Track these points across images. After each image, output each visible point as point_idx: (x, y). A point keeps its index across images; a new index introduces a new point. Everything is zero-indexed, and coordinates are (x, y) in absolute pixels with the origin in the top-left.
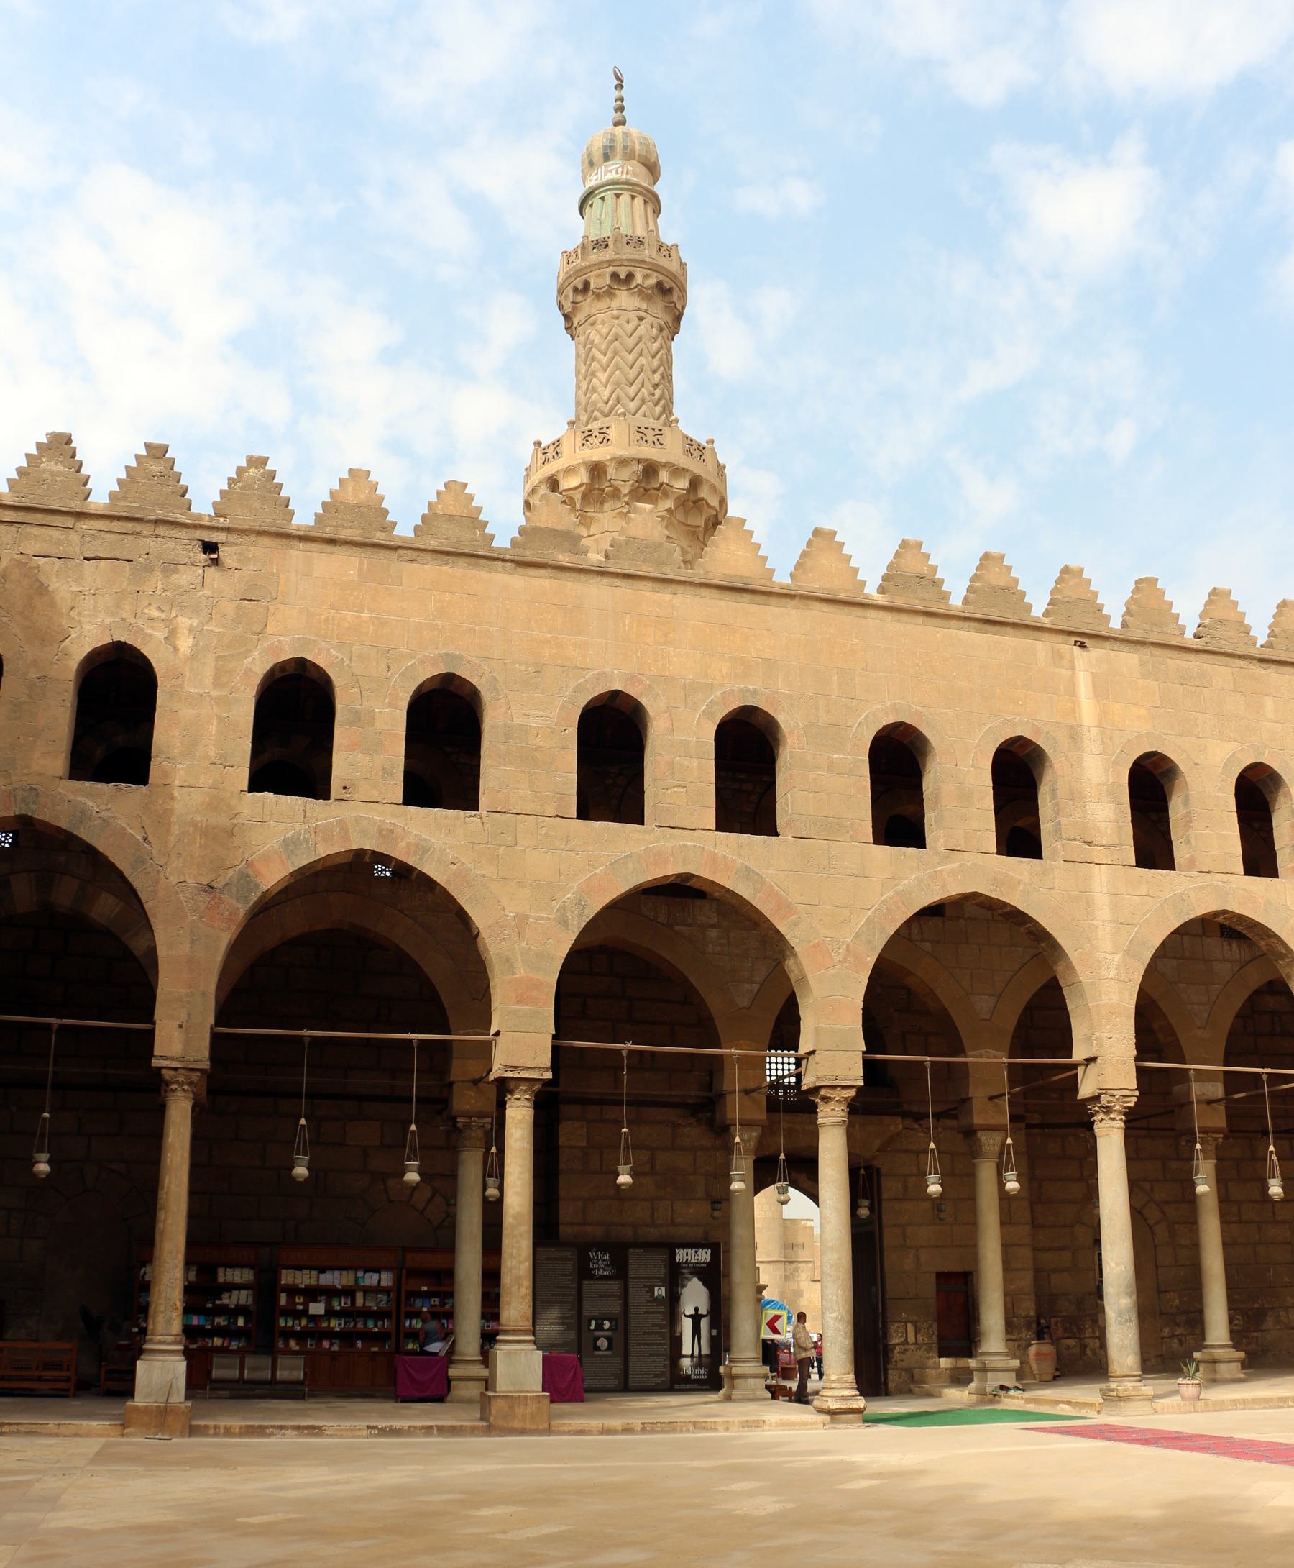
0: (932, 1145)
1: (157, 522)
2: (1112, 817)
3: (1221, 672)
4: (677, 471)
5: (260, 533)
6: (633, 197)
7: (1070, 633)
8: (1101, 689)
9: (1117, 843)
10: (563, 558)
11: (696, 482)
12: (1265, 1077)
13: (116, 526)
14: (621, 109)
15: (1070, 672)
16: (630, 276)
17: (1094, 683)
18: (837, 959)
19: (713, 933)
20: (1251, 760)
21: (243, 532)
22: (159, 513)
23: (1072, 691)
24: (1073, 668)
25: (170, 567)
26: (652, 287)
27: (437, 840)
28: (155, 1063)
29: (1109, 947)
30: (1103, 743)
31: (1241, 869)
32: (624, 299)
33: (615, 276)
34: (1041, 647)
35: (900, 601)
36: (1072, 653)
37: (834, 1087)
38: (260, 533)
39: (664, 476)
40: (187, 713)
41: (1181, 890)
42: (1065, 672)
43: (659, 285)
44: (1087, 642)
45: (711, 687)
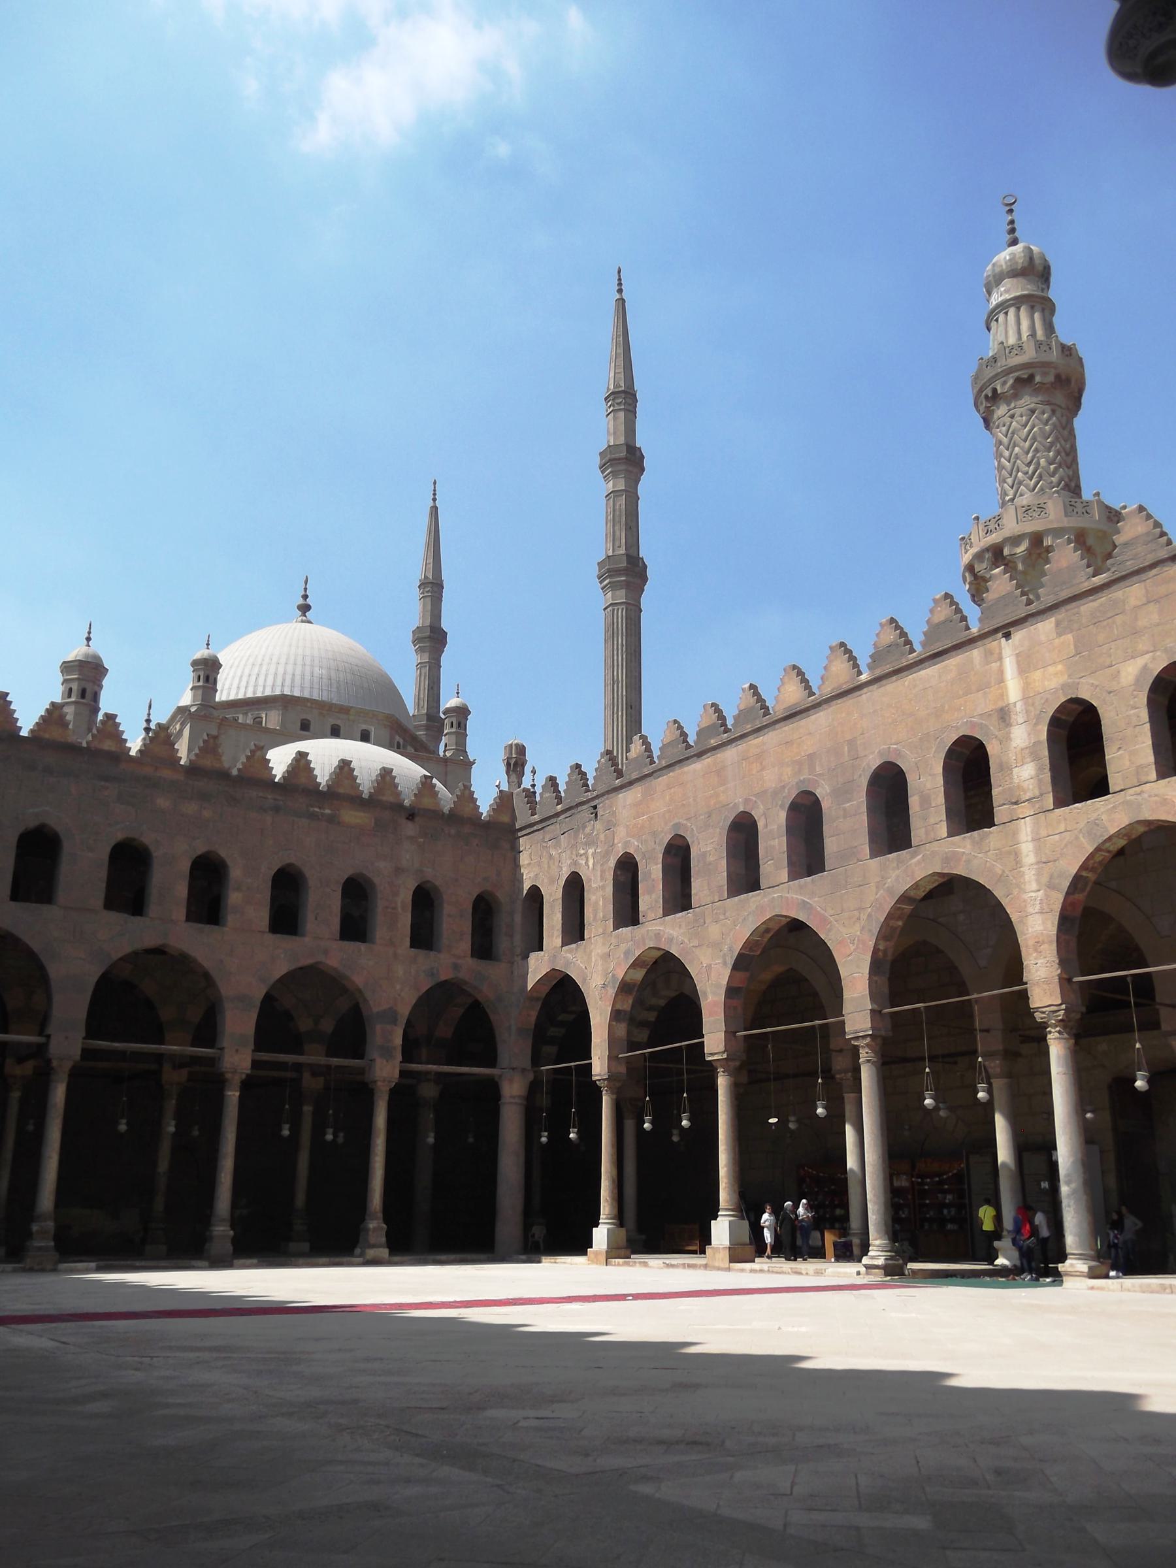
0: (927, 1070)
1: (578, 805)
2: (1033, 773)
4: (1015, 540)
5: (608, 792)
6: (1018, 309)
7: (996, 631)
8: (1025, 665)
9: (1037, 793)
10: (713, 742)
11: (1037, 539)
13: (567, 814)
14: (1013, 231)
15: (998, 664)
16: (995, 390)
17: (1018, 663)
18: (852, 947)
19: (961, 917)
21: (602, 795)
22: (578, 800)
23: (1001, 680)
24: (1000, 659)
25: (584, 827)
26: (1013, 387)
27: (675, 934)
28: (594, 1078)
29: (1034, 886)
32: (1001, 410)
33: (986, 397)
34: (975, 654)
35: (878, 672)
36: (1000, 648)
37: (857, 1038)
38: (608, 792)
39: (1006, 552)
40: (593, 898)
41: (1095, 815)
42: (995, 666)
43: (1018, 380)
45: (784, 787)
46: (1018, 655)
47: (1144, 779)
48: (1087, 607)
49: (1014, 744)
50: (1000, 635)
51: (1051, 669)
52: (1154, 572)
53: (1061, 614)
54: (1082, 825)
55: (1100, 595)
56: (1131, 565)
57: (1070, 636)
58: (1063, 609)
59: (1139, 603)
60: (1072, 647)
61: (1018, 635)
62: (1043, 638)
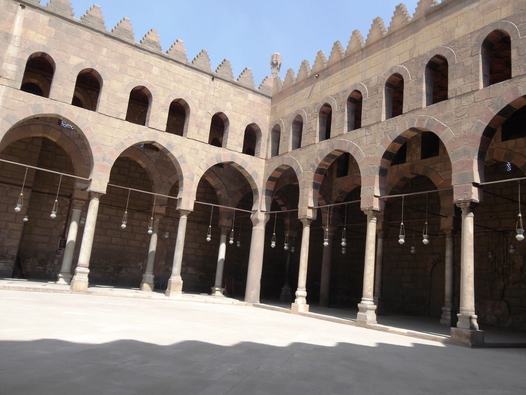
3: (87, 35)
12: (27, 168)
15: (13, 14)
17: (24, 21)
20: (88, 66)
24: (15, 13)
30: (21, 43)
31: (71, 102)
41: (39, 103)
42: (11, 14)
44: (26, 6)
46: (25, 19)
47: (66, 101)
48: (65, 25)
49: (8, 52)
50: (19, 4)
51: (40, 35)
52: (97, 33)
53: (54, 18)
54: (33, 103)
55: (73, 24)
56: (90, 25)
57: (54, 29)
58: (54, 17)
59: (87, 39)
60: (53, 34)
61: (28, 11)
62: (41, 21)
